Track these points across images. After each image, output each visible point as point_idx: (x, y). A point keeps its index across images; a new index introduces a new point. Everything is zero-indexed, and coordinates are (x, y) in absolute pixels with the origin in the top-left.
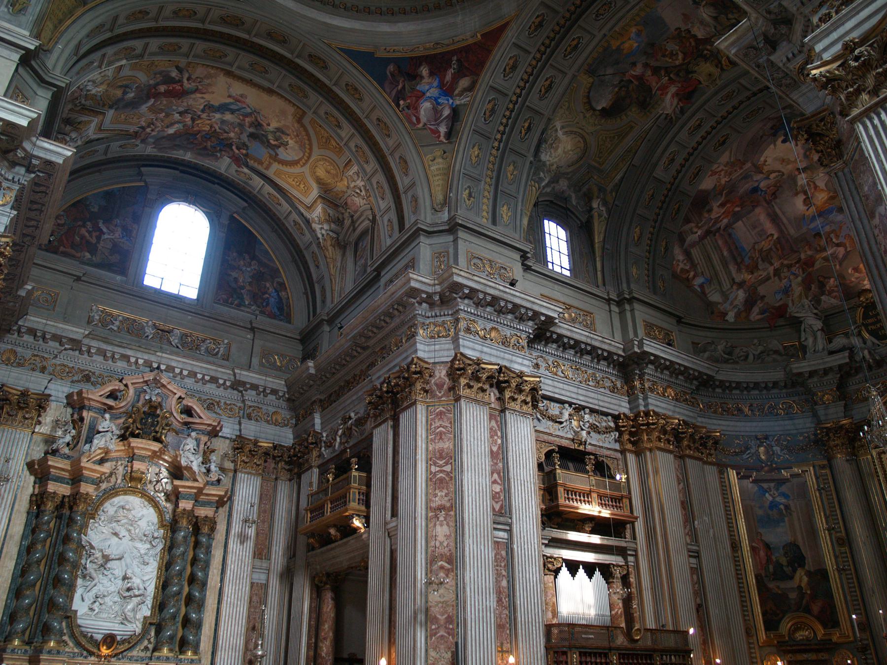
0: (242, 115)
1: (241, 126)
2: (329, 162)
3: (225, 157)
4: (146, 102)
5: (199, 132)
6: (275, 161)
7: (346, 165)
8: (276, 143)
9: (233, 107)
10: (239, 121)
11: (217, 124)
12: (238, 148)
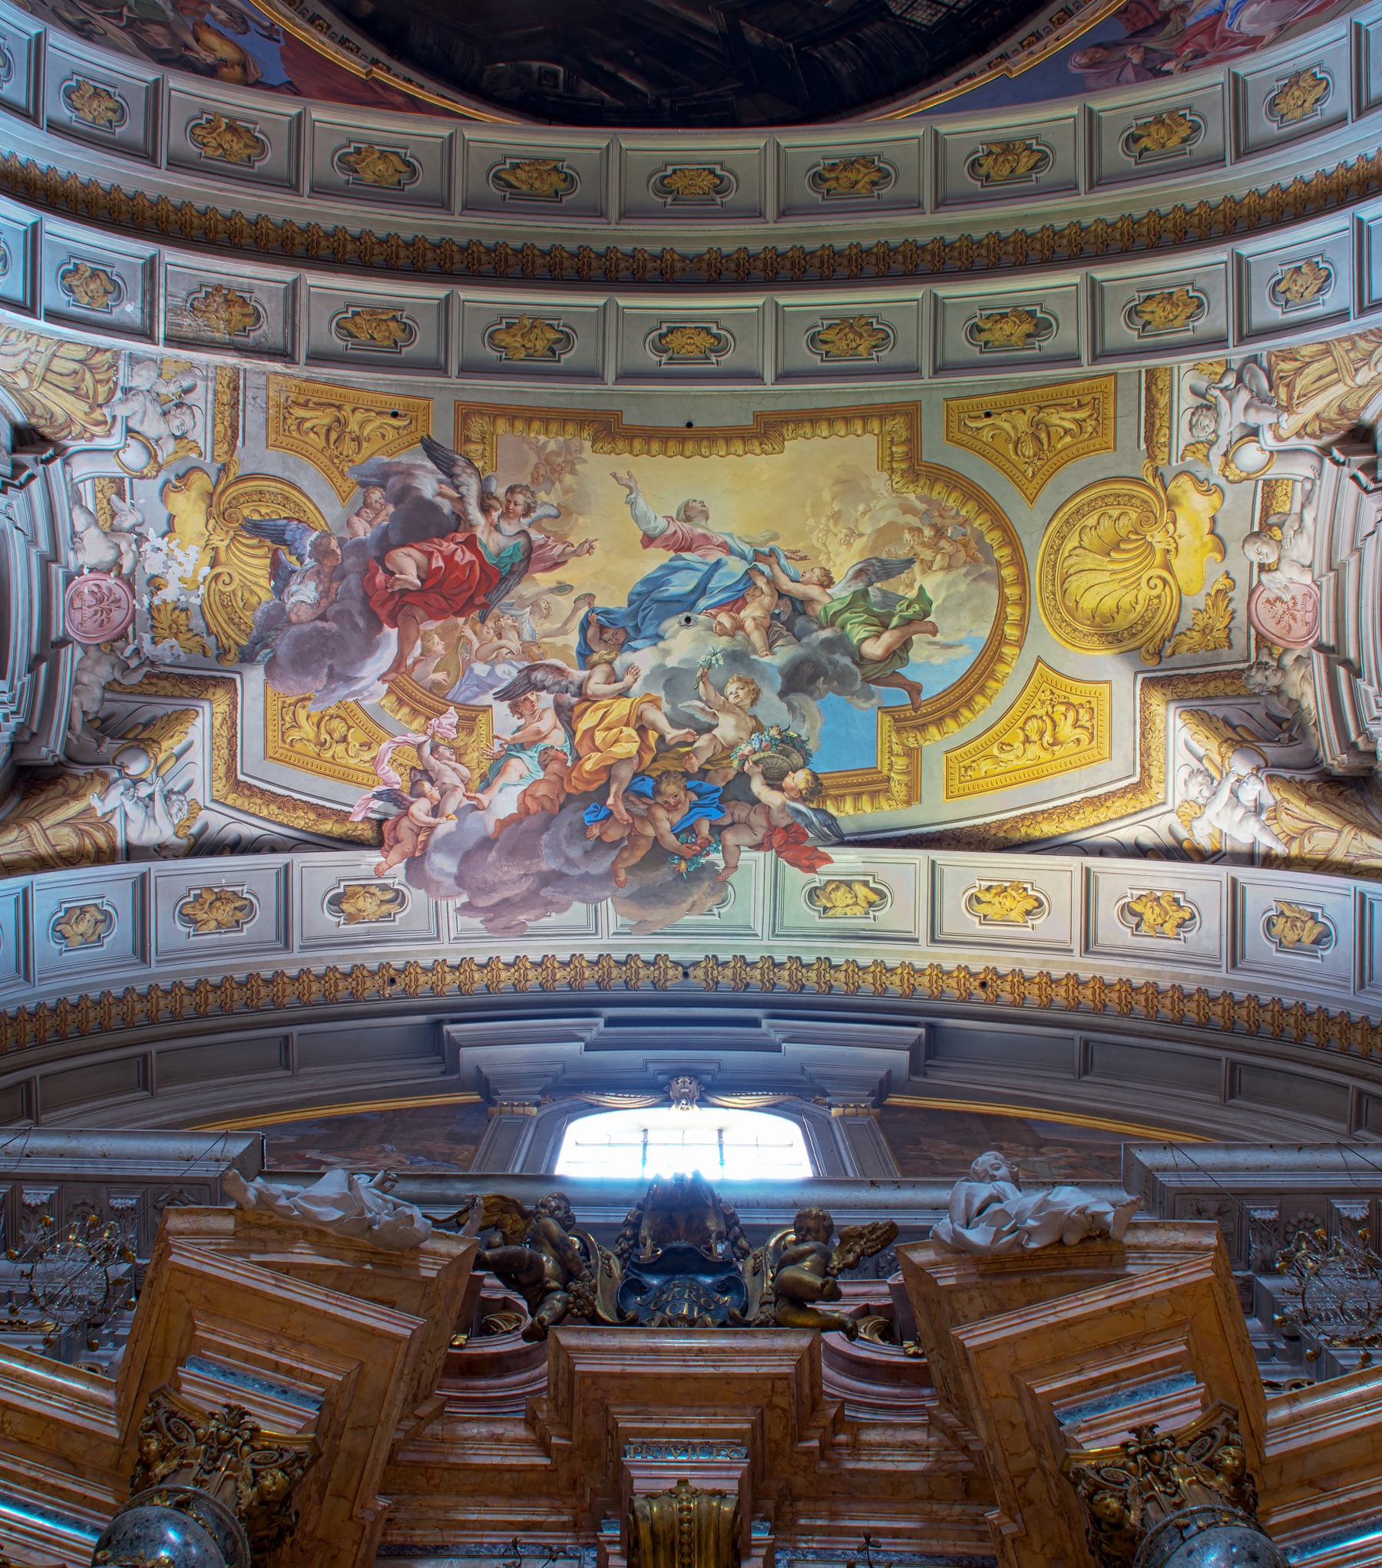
0: (720, 606)
1: (738, 658)
2: (1092, 506)
3: (747, 856)
4: (369, 648)
5: (608, 771)
6: (922, 728)
7: (1149, 440)
8: (887, 638)
9: (681, 584)
10: (723, 642)
11: (655, 702)
12: (774, 781)
